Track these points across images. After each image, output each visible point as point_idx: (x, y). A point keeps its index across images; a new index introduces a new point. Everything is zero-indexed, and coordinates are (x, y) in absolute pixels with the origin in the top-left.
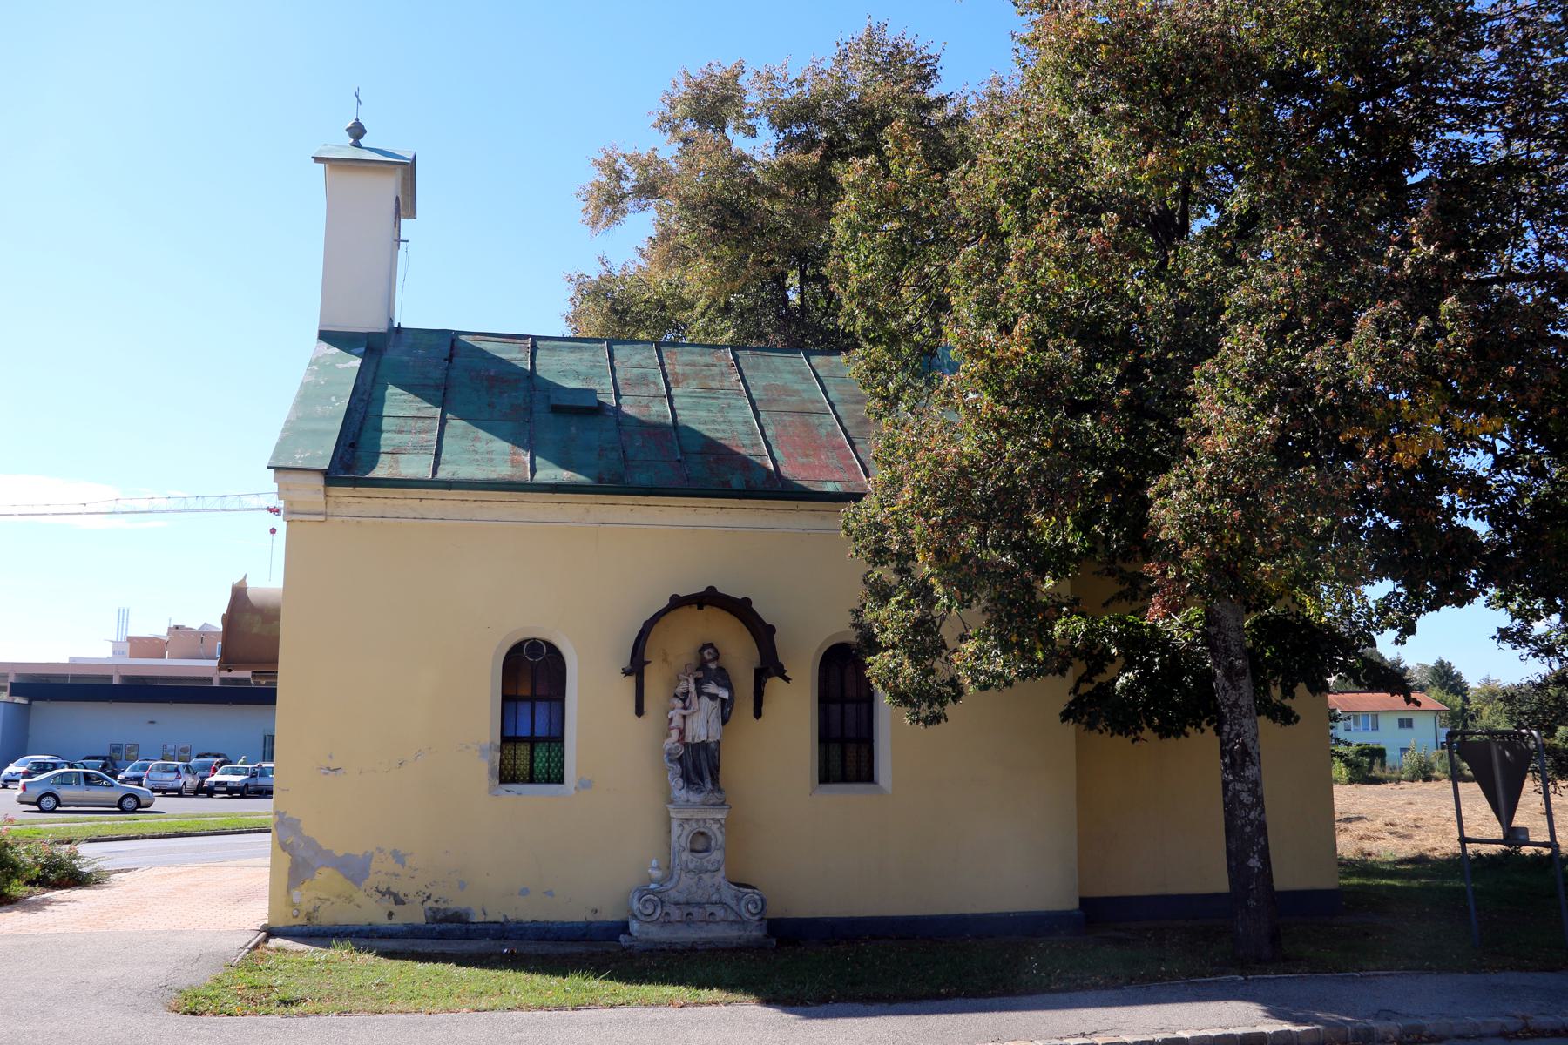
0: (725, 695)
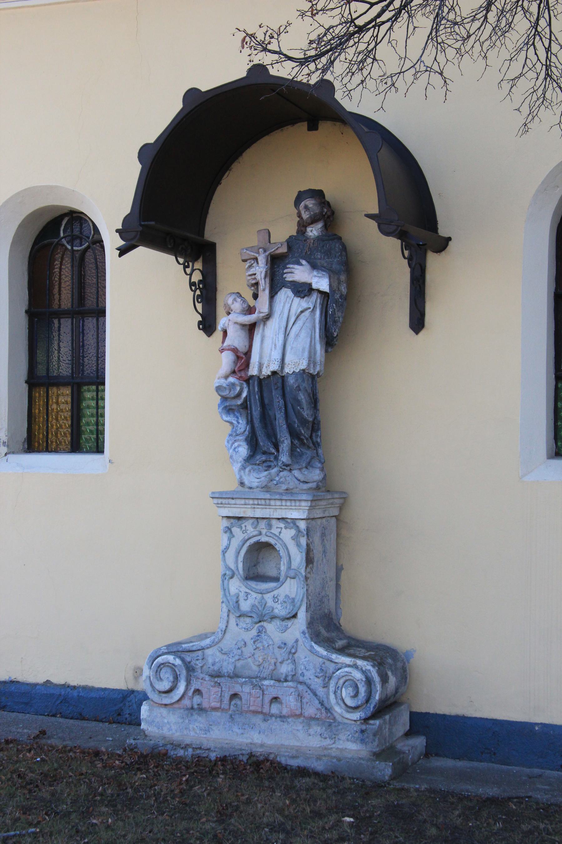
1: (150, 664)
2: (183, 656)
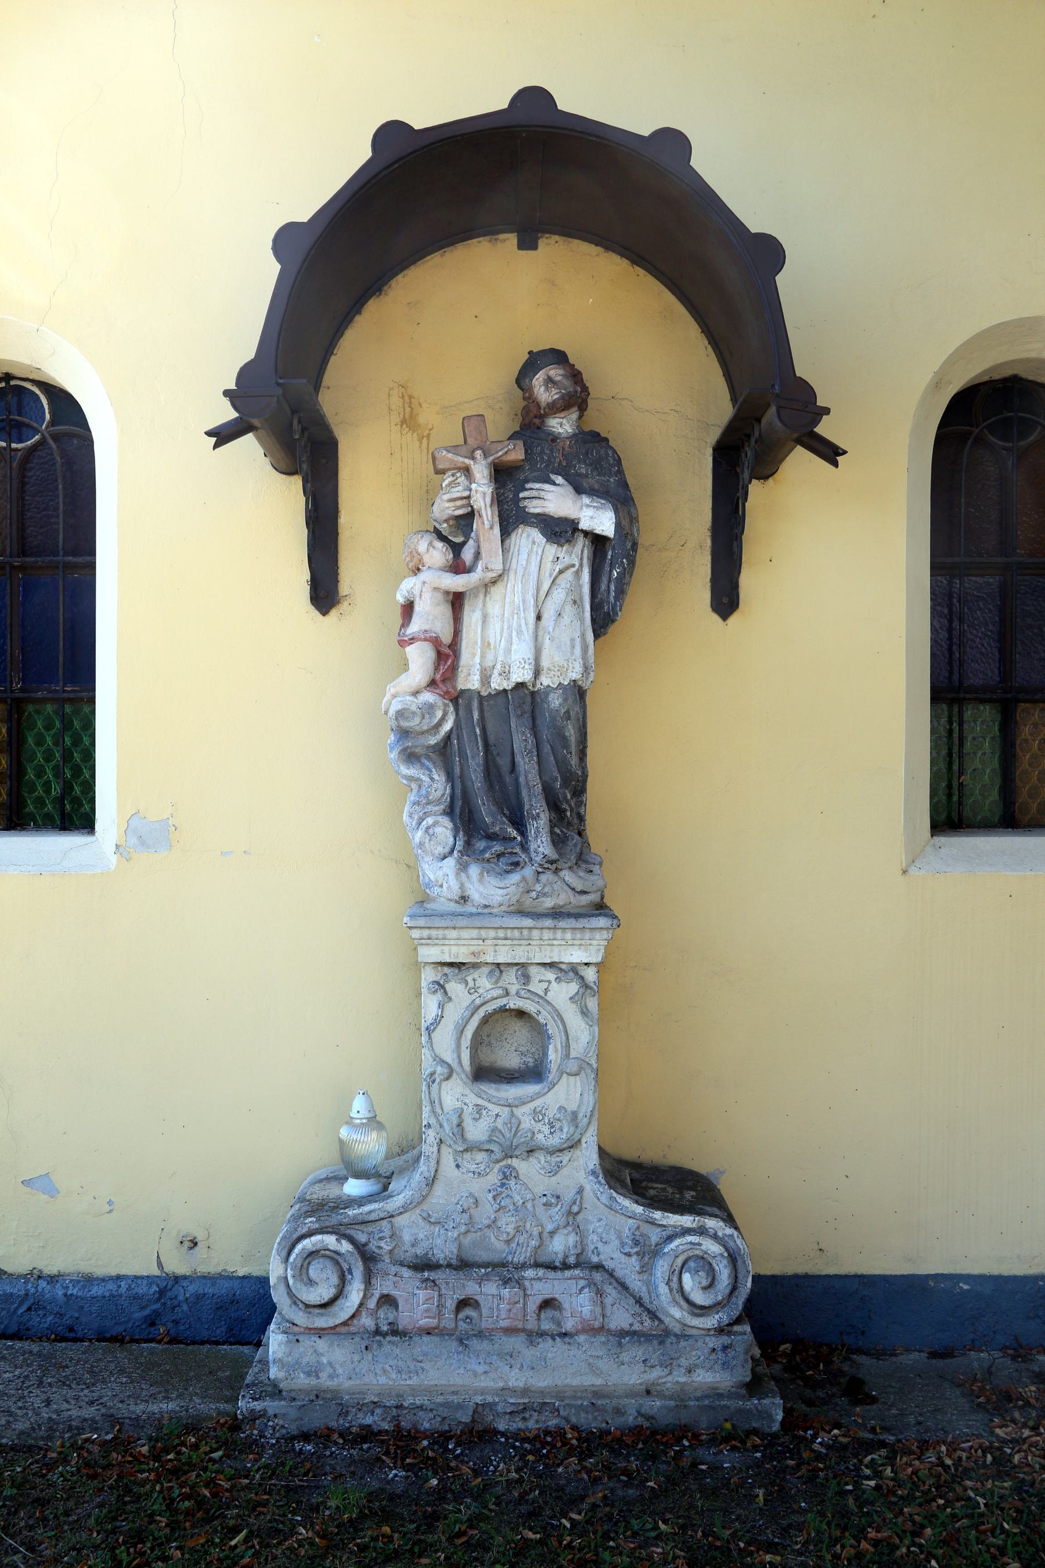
0: (602, 521)
1: (284, 1253)
2: (348, 1232)
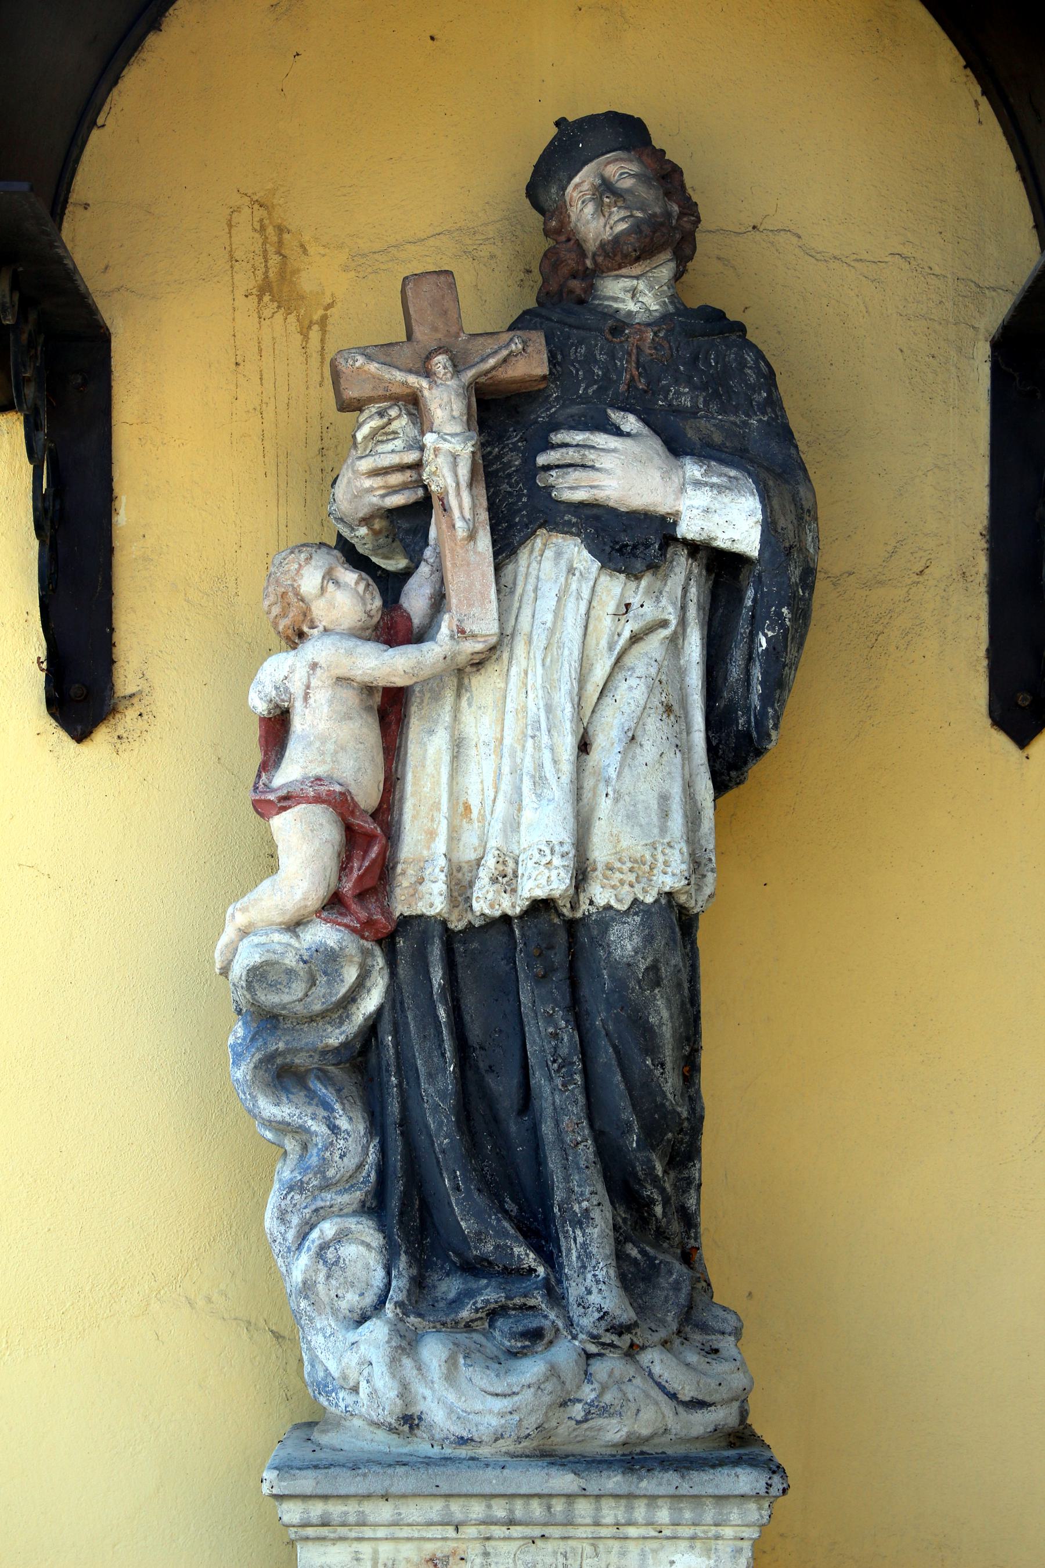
0: (731, 518)
